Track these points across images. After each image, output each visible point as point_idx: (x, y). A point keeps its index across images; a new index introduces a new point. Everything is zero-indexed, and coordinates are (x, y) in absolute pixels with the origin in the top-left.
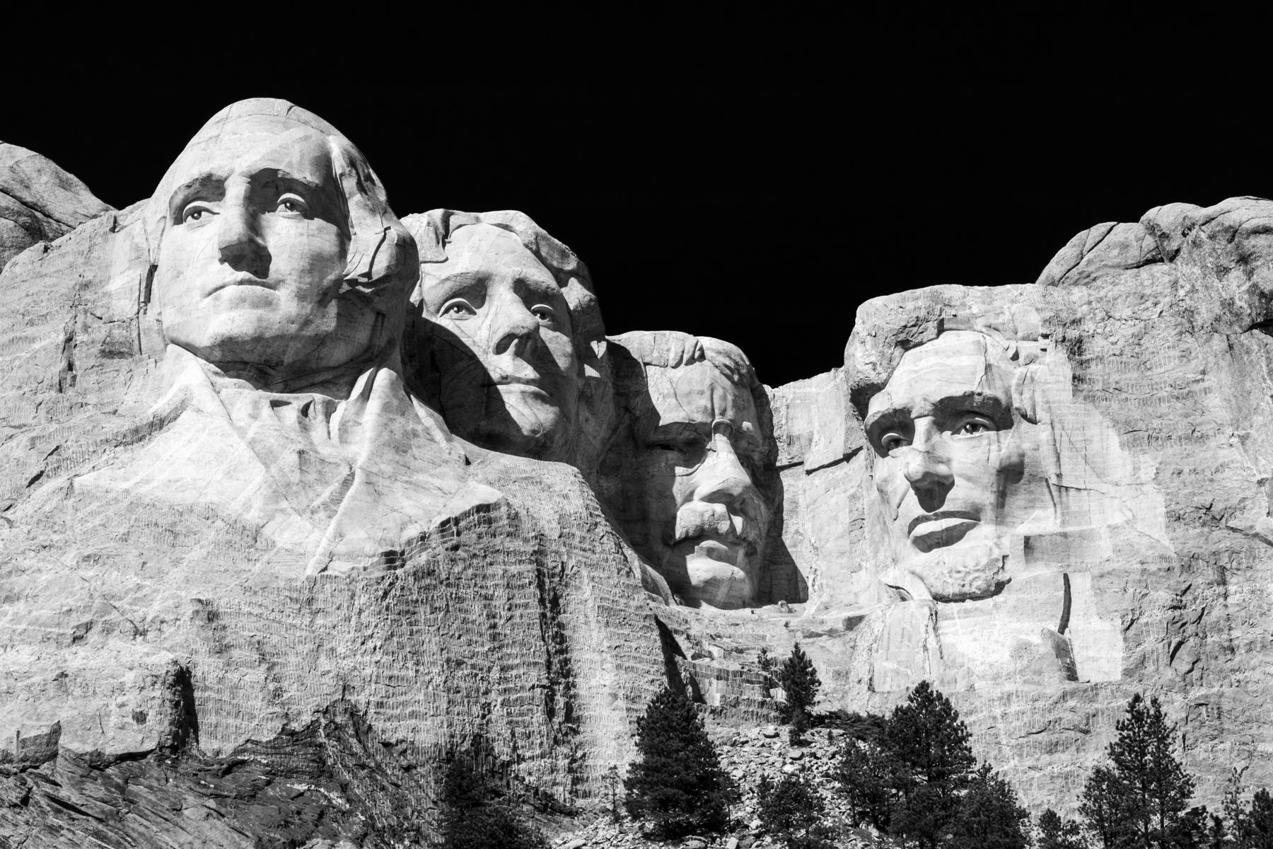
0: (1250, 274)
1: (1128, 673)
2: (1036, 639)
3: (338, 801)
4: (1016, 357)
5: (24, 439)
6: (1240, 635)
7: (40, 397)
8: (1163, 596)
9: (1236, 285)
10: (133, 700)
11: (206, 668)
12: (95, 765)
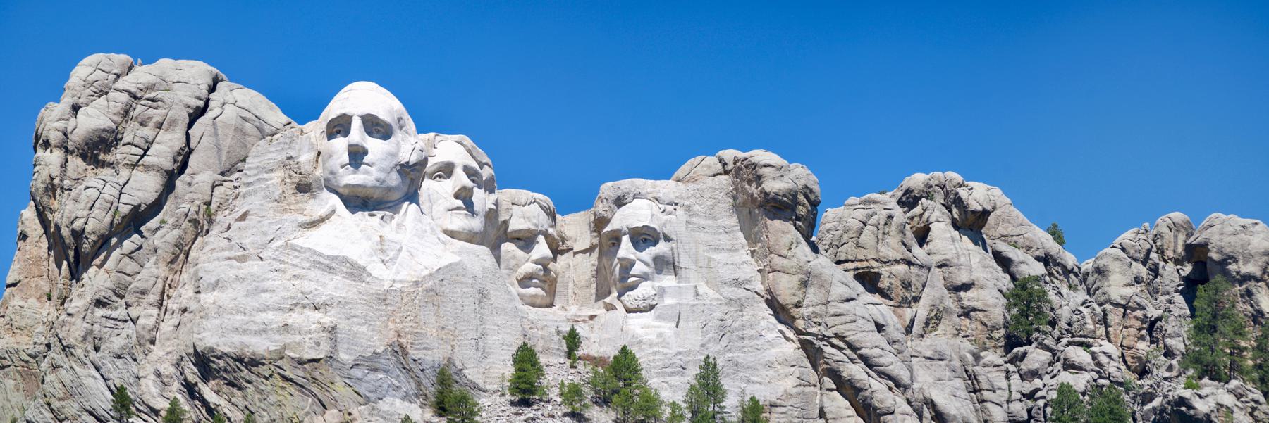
0: (759, 185)
1: (702, 346)
2: (666, 330)
3: (396, 383)
5: (266, 222)
6: (748, 332)
8: (719, 315)
9: (753, 189)
10: (314, 336)
11: (343, 325)
12: (301, 362)
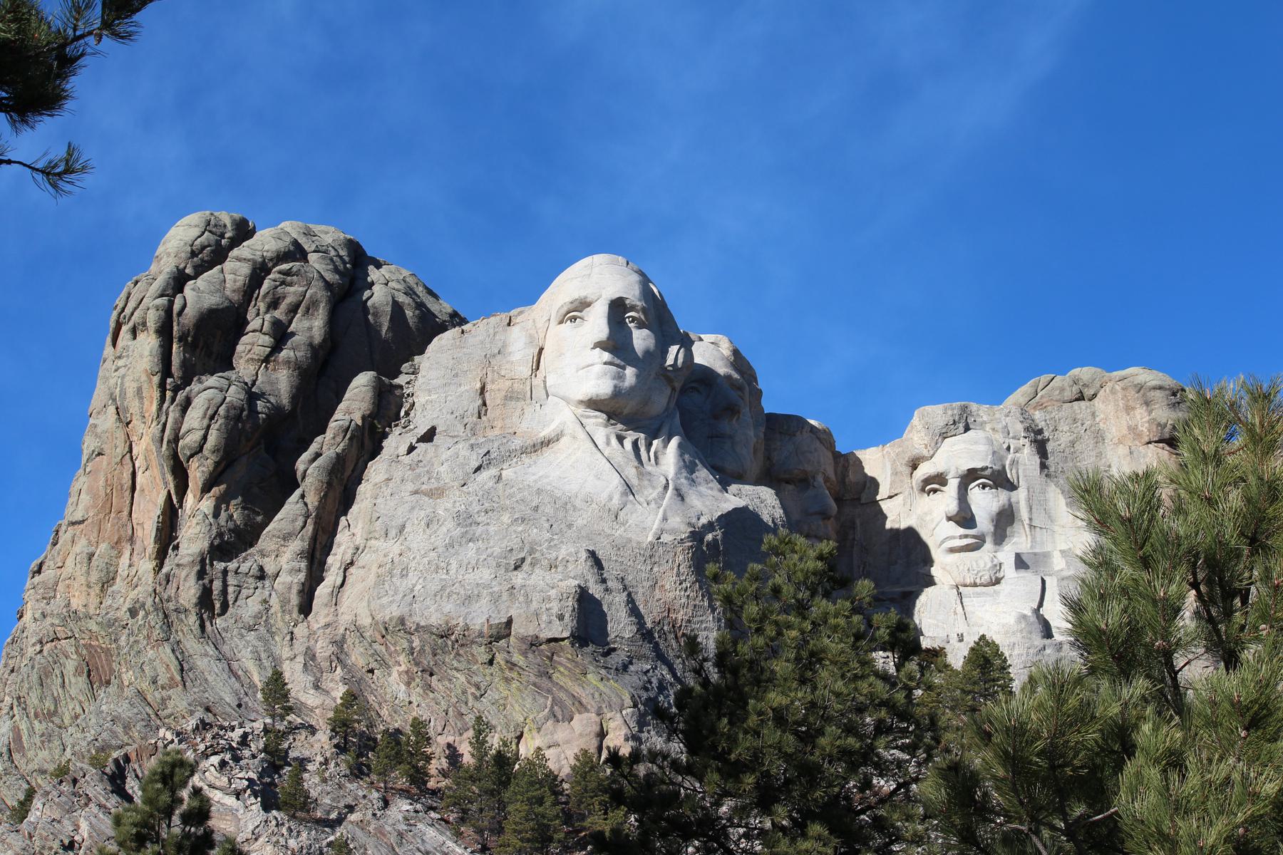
0: (1150, 412)
4: (1008, 448)
7: (466, 420)
12: (533, 644)
